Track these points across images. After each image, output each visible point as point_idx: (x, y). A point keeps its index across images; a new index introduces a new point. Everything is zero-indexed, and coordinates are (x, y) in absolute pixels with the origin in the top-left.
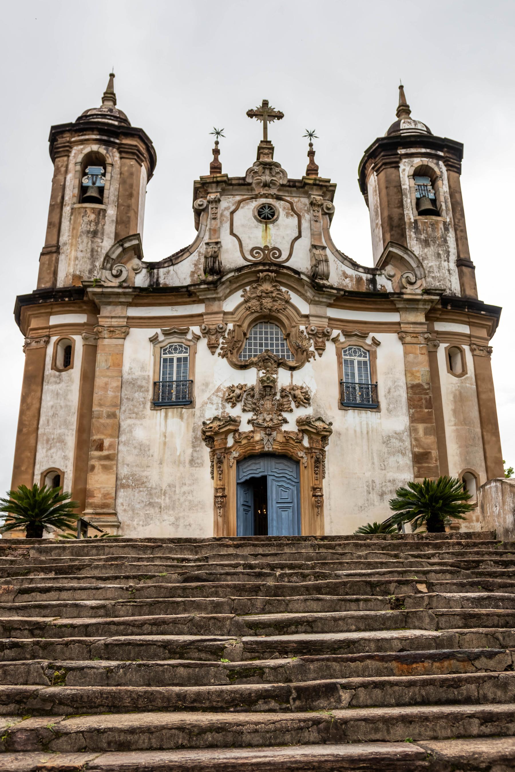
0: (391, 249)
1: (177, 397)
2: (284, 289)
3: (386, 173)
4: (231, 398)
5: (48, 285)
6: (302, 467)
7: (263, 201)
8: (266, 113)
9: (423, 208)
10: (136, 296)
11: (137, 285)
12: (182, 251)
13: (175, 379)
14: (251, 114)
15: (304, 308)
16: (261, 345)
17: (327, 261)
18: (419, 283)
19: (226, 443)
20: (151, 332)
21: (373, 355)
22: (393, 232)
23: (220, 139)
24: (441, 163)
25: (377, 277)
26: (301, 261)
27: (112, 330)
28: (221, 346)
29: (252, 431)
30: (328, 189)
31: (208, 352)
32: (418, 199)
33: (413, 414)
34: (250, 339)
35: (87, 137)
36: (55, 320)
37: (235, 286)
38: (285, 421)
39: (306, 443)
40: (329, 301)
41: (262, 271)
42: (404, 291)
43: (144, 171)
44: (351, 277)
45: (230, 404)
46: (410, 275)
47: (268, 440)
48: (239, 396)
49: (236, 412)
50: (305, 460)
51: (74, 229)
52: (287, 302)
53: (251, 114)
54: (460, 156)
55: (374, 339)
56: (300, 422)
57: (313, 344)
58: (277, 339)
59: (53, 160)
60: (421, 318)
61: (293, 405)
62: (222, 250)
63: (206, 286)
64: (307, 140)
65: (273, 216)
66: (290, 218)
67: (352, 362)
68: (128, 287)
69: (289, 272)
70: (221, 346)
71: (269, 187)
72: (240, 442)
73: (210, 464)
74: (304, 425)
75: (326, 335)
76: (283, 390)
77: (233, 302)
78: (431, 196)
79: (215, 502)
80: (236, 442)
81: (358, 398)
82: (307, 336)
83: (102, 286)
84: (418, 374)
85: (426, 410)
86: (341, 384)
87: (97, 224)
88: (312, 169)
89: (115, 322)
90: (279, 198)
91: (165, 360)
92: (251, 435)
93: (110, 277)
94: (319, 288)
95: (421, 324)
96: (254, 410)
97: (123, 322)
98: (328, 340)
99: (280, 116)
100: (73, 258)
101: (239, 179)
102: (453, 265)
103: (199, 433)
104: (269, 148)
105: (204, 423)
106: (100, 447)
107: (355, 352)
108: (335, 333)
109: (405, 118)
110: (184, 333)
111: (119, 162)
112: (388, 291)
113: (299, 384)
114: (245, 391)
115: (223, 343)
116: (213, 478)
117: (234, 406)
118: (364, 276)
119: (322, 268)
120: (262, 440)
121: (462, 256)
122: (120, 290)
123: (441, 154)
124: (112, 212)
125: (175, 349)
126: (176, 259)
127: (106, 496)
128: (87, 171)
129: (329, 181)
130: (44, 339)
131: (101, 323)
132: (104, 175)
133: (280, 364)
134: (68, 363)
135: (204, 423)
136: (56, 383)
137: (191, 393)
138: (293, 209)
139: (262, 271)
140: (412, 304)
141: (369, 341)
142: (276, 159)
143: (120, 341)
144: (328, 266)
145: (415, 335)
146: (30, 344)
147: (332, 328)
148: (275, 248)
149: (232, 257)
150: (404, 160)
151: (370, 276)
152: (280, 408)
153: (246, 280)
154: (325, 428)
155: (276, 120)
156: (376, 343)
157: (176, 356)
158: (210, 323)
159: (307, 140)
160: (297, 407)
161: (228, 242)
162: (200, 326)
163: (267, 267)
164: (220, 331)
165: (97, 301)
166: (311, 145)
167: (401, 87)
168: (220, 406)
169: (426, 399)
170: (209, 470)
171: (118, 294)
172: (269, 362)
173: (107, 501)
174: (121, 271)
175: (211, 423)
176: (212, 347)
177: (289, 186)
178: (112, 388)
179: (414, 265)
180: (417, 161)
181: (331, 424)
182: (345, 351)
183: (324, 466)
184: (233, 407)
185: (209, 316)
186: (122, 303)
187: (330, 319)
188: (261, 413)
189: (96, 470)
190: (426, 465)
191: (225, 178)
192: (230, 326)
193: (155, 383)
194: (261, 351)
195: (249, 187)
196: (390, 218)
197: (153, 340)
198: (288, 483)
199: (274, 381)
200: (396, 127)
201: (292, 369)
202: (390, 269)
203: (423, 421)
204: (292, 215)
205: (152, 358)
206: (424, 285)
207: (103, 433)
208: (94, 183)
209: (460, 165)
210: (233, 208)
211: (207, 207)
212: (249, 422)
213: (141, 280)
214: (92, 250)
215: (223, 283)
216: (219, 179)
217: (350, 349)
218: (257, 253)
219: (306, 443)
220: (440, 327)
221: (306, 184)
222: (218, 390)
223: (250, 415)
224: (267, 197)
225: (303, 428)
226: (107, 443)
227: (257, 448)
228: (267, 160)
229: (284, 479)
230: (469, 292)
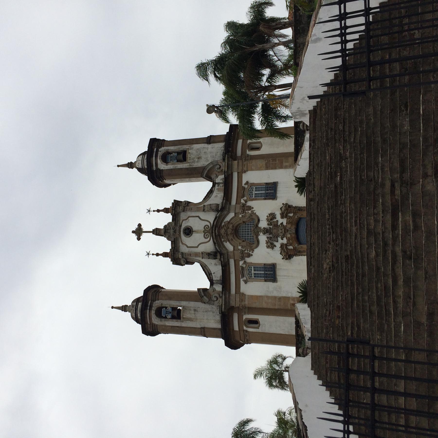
0: (204, 176)
1: (271, 271)
2: (223, 224)
5: (220, 332)
6: (302, 216)
7: (182, 233)
8: (139, 232)
11: (221, 290)
12: (204, 270)
13: (263, 272)
14: (139, 239)
15: (232, 215)
16: (248, 234)
17: (210, 205)
18: (220, 164)
20: (242, 283)
21: (253, 184)
23: (151, 253)
24: (160, 150)
26: (211, 217)
27: (242, 300)
28: (248, 252)
30: (176, 203)
31: (251, 257)
32: (177, 161)
34: (245, 239)
36: (236, 328)
37: (222, 245)
38: (282, 223)
39: (291, 215)
41: (215, 233)
42: (223, 171)
43: (162, 290)
45: (275, 247)
46: (216, 167)
49: (278, 245)
50: (299, 215)
52: (229, 222)
53: (139, 239)
55: (245, 184)
56: (282, 217)
58: (245, 227)
60: (236, 162)
61: (275, 220)
62: (205, 251)
64: (152, 213)
65: (188, 229)
67: (256, 194)
68: (222, 293)
70: (248, 252)
73: (301, 256)
75: (244, 205)
76: (268, 224)
77: (229, 247)
78: (176, 154)
80: (291, 245)
81: (272, 192)
83: (222, 305)
84: (261, 165)
86: (265, 199)
88: (166, 210)
89: (238, 299)
91: (255, 277)
93: (218, 301)
94: (223, 209)
95: (238, 163)
96: (277, 237)
97: (238, 296)
99: (140, 225)
101: (172, 244)
102: (210, 146)
103: (287, 261)
105: (283, 259)
107: (251, 192)
108: (242, 201)
110: (243, 268)
111: (160, 301)
112: (224, 177)
113: (266, 217)
117: (275, 246)
119: (214, 208)
120: (290, 234)
121: (205, 141)
123: (155, 149)
124: (184, 303)
125: (250, 272)
132: (166, 308)
133: (257, 226)
135: (283, 259)
137: (270, 265)
138: (186, 220)
139: (215, 233)
140: (230, 167)
141: (246, 186)
142: (162, 227)
143: (246, 297)
144: (213, 204)
147: (240, 203)
148: (204, 228)
149: (209, 247)
150: (159, 167)
151: (216, 185)
152: (276, 225)
155: (142, 227)
156: (247, 183)
159: (152, 213)
160: (276, 218)
161: (201, 249)
162: (240, 261)
163: (214, 231)
164: (242, 252)
166: (154, 211)
167: (118, 166)
169: (272, 161)
171: (225, 298)
172: (257, 230)
176: (249, 256)
179: (212, 166)
180: (159, 161)
181: (283, 204)
182: (251, 197)
183: (302, 207)
184: (276, 246)
186: (229, 296)
187: (236, 203)
192: (240, 247)
193: (265, 281)
194: (251, 234)
197: (246, 282)
199: (264, 228)
200: (141, 170)
201: (259, 220)
202: (213, 176)
203: (282, 163)
205: (254, 282)
208: (170, 313)
210: (185, 246)
211: (184, 258)
212: (282, 239)
213: (219, 288)
214: (204, 312)
215: (221, 251)
219: (291, 215)
220: (239, 153)
223: (279, 239)
224: (180, 231)
226: (292, 302)
228: (162, 232)
230: (222, 139)
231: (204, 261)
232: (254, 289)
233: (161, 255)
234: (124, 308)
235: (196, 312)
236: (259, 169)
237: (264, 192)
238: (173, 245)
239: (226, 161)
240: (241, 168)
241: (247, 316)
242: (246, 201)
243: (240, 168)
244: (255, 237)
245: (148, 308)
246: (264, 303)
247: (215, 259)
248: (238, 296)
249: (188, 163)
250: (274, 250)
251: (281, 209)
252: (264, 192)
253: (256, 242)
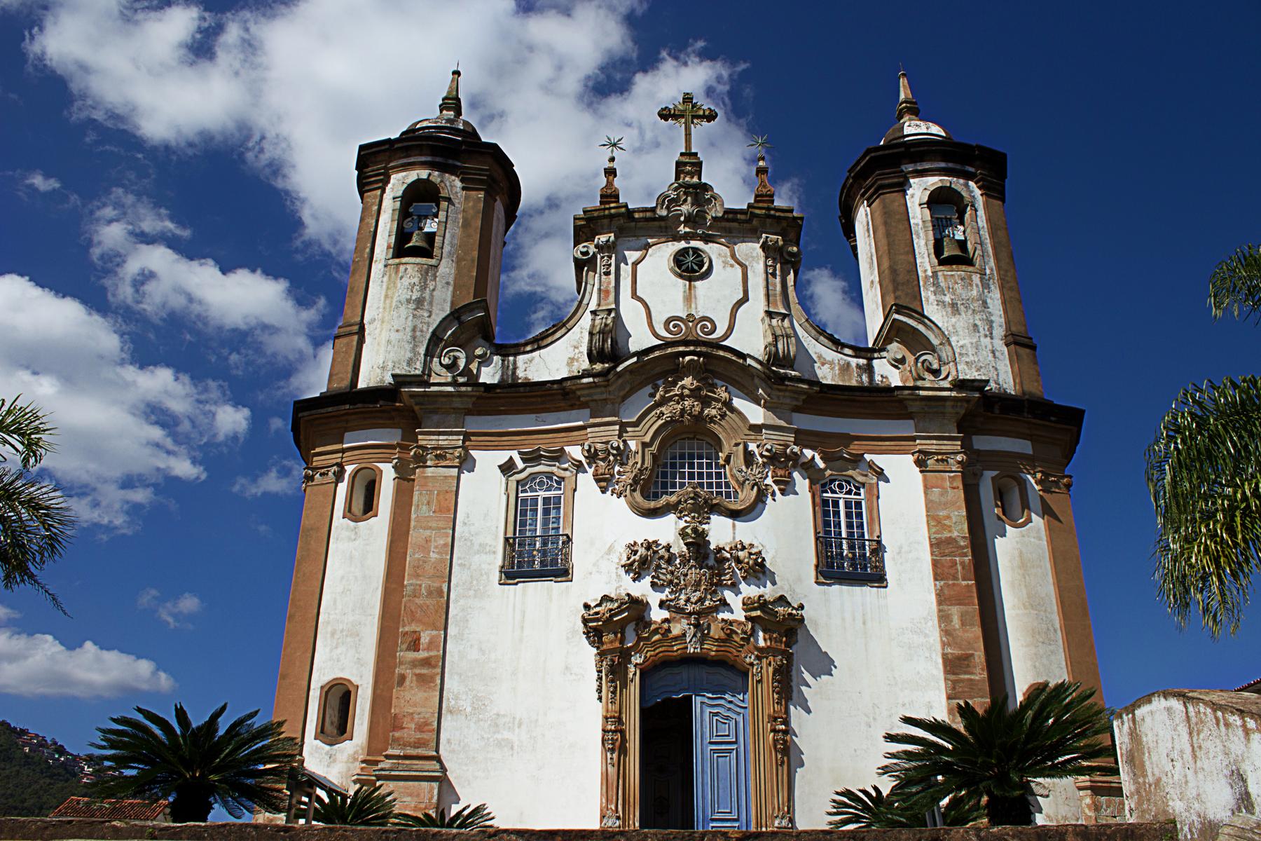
3: (883, 202)
4: (631, 564)
5: (345, 384)
9: (946, 254)
10: (478, 398)
14: (665, 115)
15: (755, 414)
19: (622, 641)
20: (502, 456)
22: (898, 293)
25: (875, 362)
29: (666, 620)
33: (941, 590)
35: (412, 160)
38: (724, 604)
40: (795, 403)
41: (684, 354)
42: (919, 383)
43: (499, 207)
44: (831, 363)
47: (695, 635)
48: (644, 562)
51: (386, 296)
52: (728, 404)
53: (665, 115)
54: (1002, 174)
55: (871, 465)
56: (748, 605)
59: (362, 194)
63: (591, 380)
65: (701, 266)
66: (729, 269)
67: (836, 504)
69: (728, 355)
71: (695, 222)
74: (755, 609)
76: (719, 550)
78: (959, 236)
79: (603, 741)
82: (760, 460)
84: (947, 522)
85: (964, 583)
86: (817, 539)
87: (423, 288)
89: (443, 441)
90: (707, 239)
91: (524, 501)
92: (666, 626)
98: (795, 467)
100: (384, 342)
101: (645, 210)
102: (1000, 345)
104: (692, 164)
105: (587, 606)
106: (415, 645)
109: (910, 120)
114: (656, 552)
115: (619, 473)
116: (600, 699)
118: (854, 362)
121: (1014, 329)
122: (450, 389)
124: (446, 269)
125: (541, 483)
126: (543, 339)
127: (421, 727)
128: (411, 210)
129: (791, 211)
130: (335, 468)
131: (421, 443)
134: (369, 507)
135: (587, 606)
136: (350, 539)
137: (567, 557)
138: (733, 256)
139: (684, 354)
145: (944, 457)
146: (313, 476)
151: (862, 361)
153: (658, 370)
154: (790, 614)
157: (542, 494)
158: (597, 440)
162: (582, 445)
163: (692, 348)
165: (416, 408)
168: (614, 576)
169: (962, 563)
170: (595, 685)
171: (449, 394)
173: (425, 736)
174: (456, 358)
175: (597, 606)
177: (728, 220)
178: (436, 547)
179: (935, 341)
180: (933, 181)
181: (801, 607)
184: (634, 580)
185: (597, 429)
189: (407, 682)
190: (967, 677)
191: (623, 210)
193: (507, 539)
195: (663, 224)
196: (893, 271)
198: (729, 709)
201: (735, 515)
202: (896, 349)
204: (732, 266)
205: (504, 498)
206: (954, 373)
207: (420, 621)
209: (1004, 187)
211: (594, 255)
212: (662, 604)
213: (489, 375)
214: (414, 330)
216: (613, 211)
217: (832, 481)
218: (675, 326)
220: (983, 443)
221: (754, 215)
222: (610, 550)
225: (754, 614)
226: (425, 638)
229: (722, 702)
231: (586, 321)
232: (483, 493)
233: (609, 184)
234: (452, 103)
235: (412, 306)
236: (933, 519)
237: (844, 535)
238: (641, 215)
239: (954, 394)
240: (933, 448)
241: (388, 473)
242: (808, 468)
243: (932, 445)
244: (673, 499)
245: (438, 159)
246: (428, 533)
247: (590, 355)
248: (458, 440)
249: (935, 274)
250: (622, 571)
251: (782, 600)
252: (844, 535)
253: (652, 504)
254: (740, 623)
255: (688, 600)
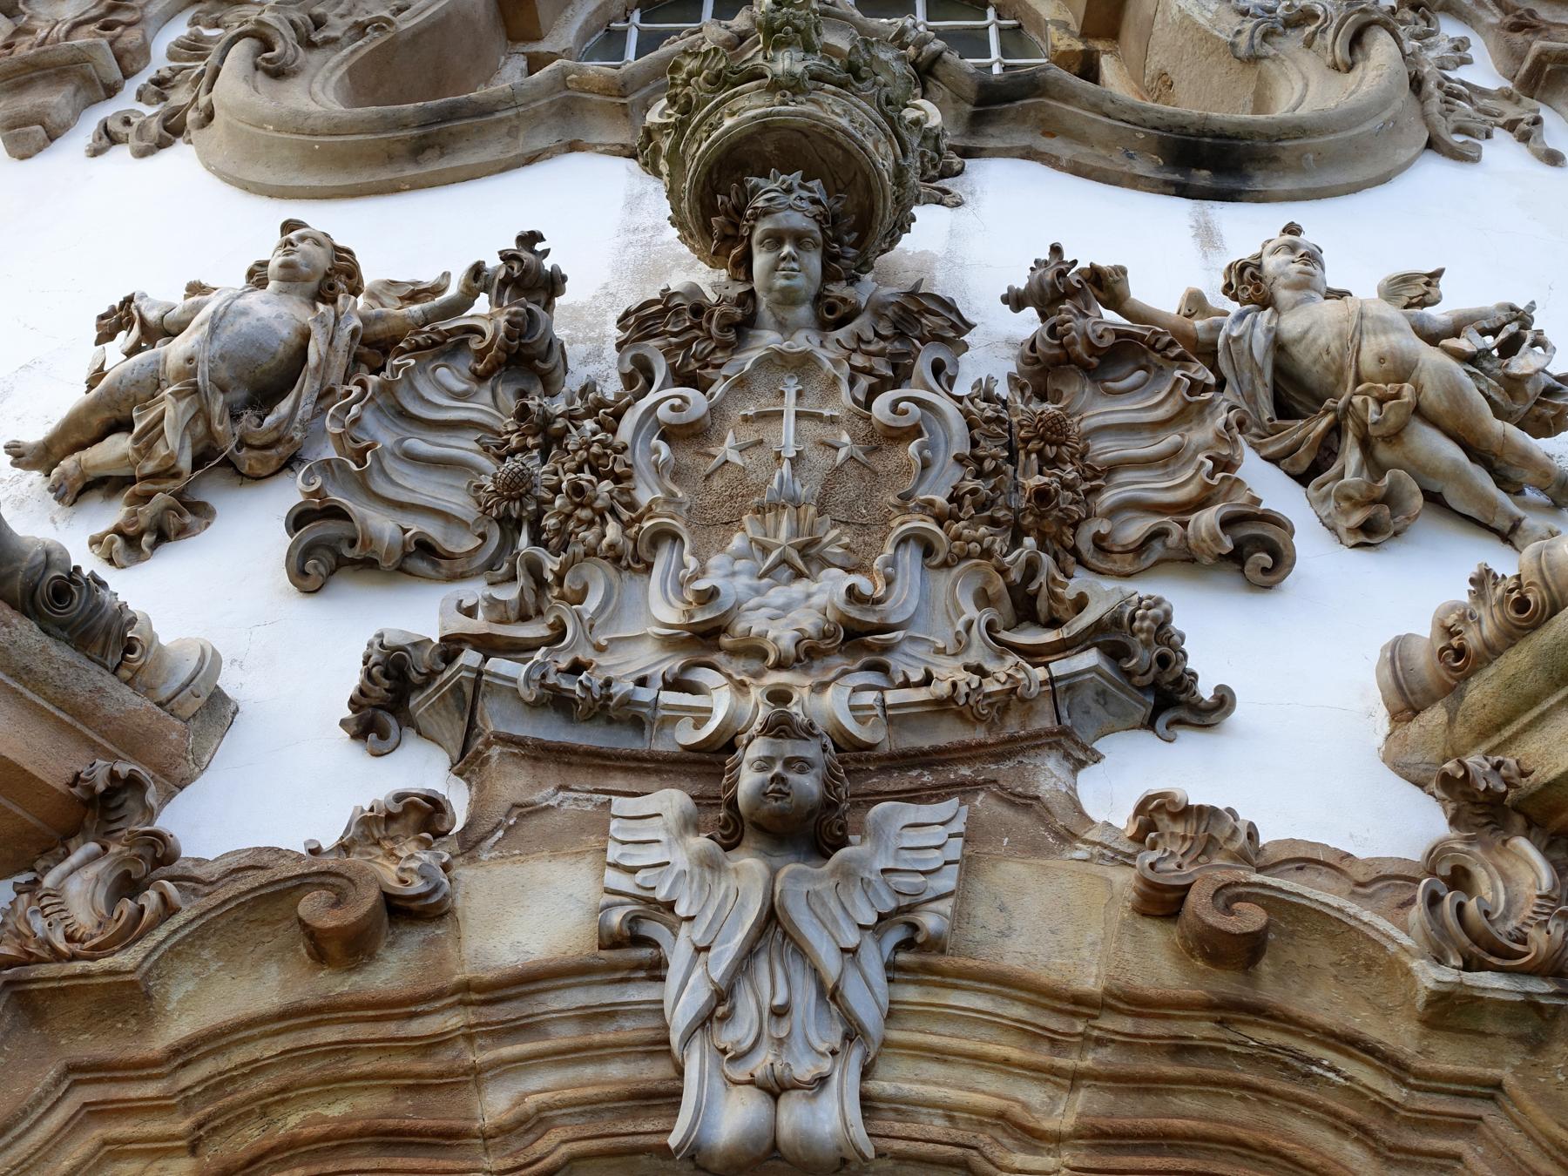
57: (1479, 48)
72: (130, 1001)
120: (631, 947)
188: (632, 562)
227: (496, 1104)
254: (1384, 881)
255: (705, 638)
